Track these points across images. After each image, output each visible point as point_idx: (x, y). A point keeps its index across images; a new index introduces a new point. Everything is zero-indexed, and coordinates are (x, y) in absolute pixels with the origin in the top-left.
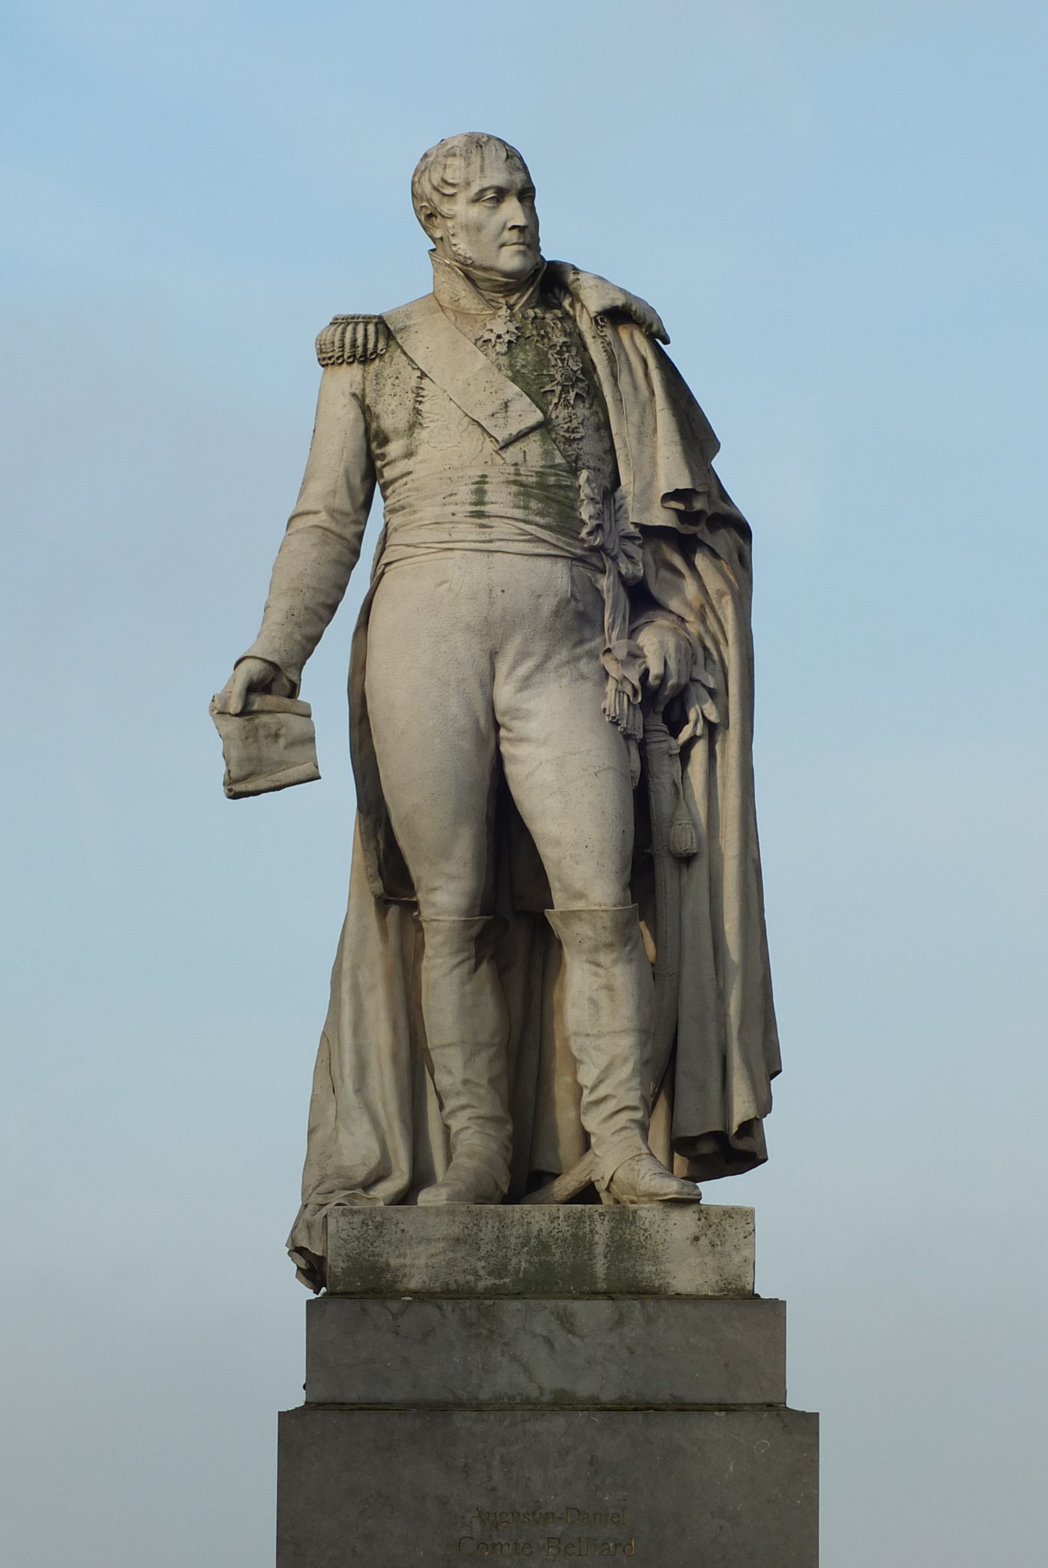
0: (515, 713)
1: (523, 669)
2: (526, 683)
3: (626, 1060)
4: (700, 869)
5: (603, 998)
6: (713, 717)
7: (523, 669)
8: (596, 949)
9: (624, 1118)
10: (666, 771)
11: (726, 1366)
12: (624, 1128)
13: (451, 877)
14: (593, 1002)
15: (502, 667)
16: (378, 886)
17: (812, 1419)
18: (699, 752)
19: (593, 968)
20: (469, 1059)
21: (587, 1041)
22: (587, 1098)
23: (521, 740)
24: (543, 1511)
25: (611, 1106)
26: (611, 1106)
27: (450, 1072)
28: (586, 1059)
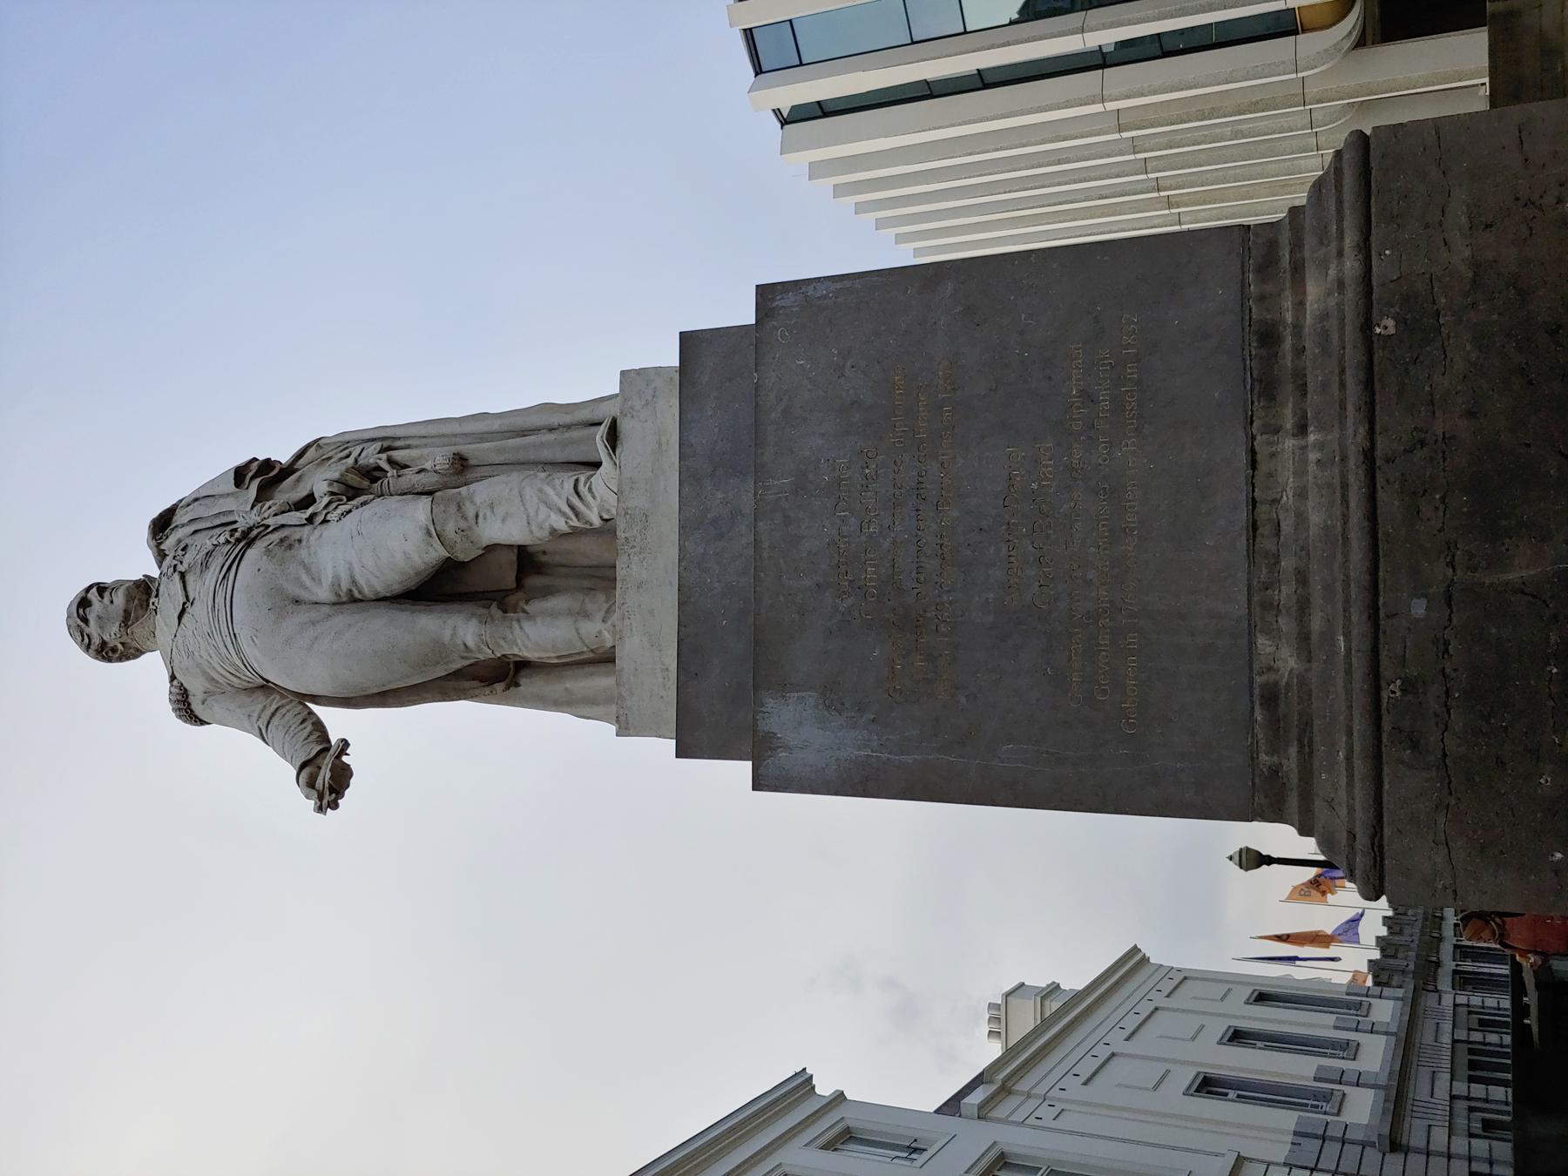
0: (336, 585)
1: (308, 582)
2: (317, 580)
3: (541, 490)
4: (465, 449)
5: (500, 511)
6: (378, 445)
7: (308, 582)
8: (464, 518)
9: (583, 489)
10: (410, 478)
11: (730, 380)
12: (590, 489)
13: (454, 635)
14: (503, 521)
15: (305, 595)
16: (499, 687)
17: (765, 294)
18: (396, 455)
19: (480, 520)
20: (587, 615)
21: (533, 523)
22: (575, 523)
23: (354, 582)
24: (837, 538)
25: (575, 501)
26: (575, 501)
27: (600, 632)
28: (546, 525)
